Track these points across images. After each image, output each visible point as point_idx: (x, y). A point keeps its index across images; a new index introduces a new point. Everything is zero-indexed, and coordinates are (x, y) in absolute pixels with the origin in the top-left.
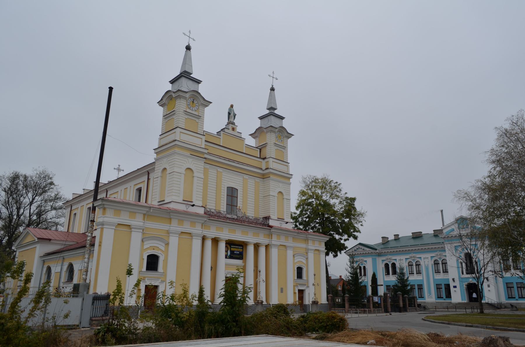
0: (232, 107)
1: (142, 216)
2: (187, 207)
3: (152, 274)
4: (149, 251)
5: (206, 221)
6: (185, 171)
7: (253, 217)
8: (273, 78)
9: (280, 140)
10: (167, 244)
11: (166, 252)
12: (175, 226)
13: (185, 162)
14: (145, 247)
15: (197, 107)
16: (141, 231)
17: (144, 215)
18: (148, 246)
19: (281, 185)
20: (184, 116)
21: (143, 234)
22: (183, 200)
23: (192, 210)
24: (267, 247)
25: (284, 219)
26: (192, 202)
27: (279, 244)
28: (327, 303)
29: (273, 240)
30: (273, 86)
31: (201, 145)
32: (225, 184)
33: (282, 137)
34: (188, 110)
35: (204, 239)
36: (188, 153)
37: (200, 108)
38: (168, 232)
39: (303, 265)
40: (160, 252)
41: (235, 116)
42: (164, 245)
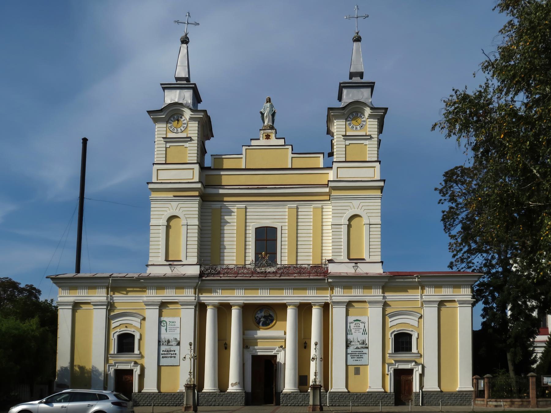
2: (173, 268)
3: (124, 357)
4: (118, 330)
7: (309, 265)
9: (358, 127)
10: (144, 319)
14: (113, 326)
15: (185, 125)
16: (105, 307)
18: (118, 324)
19: (356, 203)
24: (326, 308)
25: (364, 259)
26: (181, 261)
27: (348, 300)
28: (472, 389)
29: (334, 294)
34: (170, 135)
35: (201, 308)
36: (170, 195)
37: (189, 125)
39: (411, 329)
42: (139, 320)
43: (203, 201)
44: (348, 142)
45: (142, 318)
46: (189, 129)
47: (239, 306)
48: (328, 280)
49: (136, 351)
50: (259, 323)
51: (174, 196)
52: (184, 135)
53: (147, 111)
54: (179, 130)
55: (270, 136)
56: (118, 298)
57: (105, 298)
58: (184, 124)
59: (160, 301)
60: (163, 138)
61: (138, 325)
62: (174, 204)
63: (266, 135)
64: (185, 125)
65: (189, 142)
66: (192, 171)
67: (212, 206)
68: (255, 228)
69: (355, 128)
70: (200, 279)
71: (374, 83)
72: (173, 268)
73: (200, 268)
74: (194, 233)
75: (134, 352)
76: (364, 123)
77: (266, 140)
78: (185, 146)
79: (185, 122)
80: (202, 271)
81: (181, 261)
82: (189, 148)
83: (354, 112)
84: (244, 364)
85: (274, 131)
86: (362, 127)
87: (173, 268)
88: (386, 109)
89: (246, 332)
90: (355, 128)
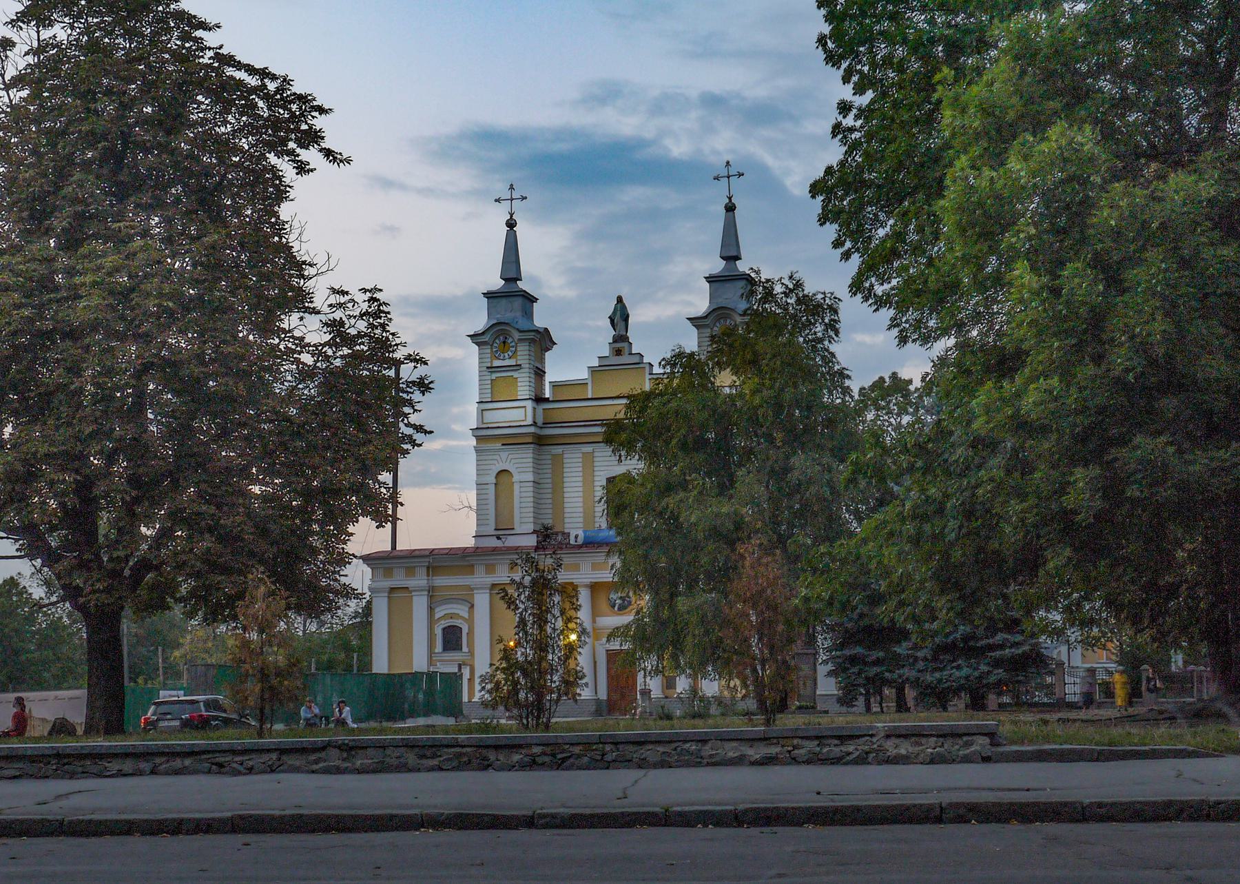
1: (425, 570)
4: (443, 622)
6: (496, 478)
10: (472, 606)
11: (470, 621)
12: (481, 578)
13: (495, 462)
14: (437, 616)
15: (514, 349)
16: (426, 593)
17: (428, 568)
20: (489, 377)
21: (431, 597)
22: (496, 529)
23: (512, 542)
30: (730, 198)
31: (525, 420)
32: (602, 473)
34: (497, 363)
36: (498, 445)
38: (470, 589)
40: (460, 621)
41: (626, 318)
42: (467, 609)
45: (470, 605)
46: (519, 353)
47: (586, 586)
49: (465, 649)
50: (613, 607)
51: (503, 445)
52: (512, 362)
54: (506, 355)
56: (440, 581)
57: (426, 581)
58: (513, 347)
59: (490, 583)
60: (488, 368)
61: (466, 616)
62: (504, 455)
64: (514, 349)
67: (553, 451)
74: (529, 488)
75: (461, 649)
79: (513, 344)
82: (519, 380)
84: (595, 663)
85: (625, 345)
89: (598, 619)
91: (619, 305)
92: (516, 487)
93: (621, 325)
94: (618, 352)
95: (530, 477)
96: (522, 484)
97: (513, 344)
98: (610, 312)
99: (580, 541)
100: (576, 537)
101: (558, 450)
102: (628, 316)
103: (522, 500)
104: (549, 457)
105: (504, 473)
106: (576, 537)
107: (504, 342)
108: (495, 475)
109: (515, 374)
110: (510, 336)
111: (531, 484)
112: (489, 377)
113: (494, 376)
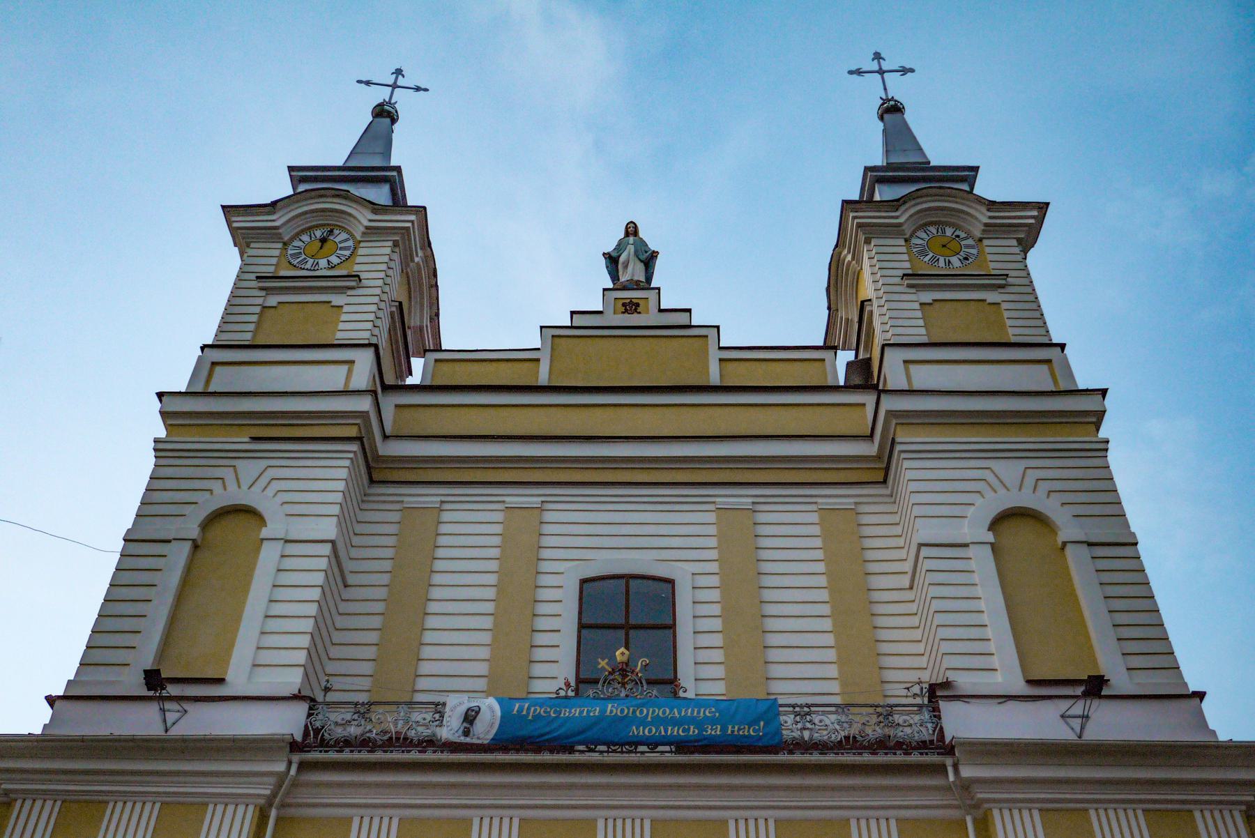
0: (636, 233)
5: (281, 777)
8: (881, 72)
15: (347, 253)
26: (221, 681)
33: (970, 242)
36: (240, 440)
41: (649, 260)
43: (372, 481)
44: (927, 297)
48: (956, 767)
51: (255, 439)
53: (223, 207)
55: (638, 305)
63: (624, 305)
64: (347, 253)
65: (350, 292)
66: (345, 368)
68: (584, 582)
69: (942, 259)
70: (296, 758)
71: (975, 169)
72: (177, 715)
73: (309, 715)
76: (974, 251)
77: (626, 315)
78: (332, 304)
80: (317, 731)
81: (221, 681)
82: (346, 309)
83: (931, 224)
85: (651, 295)
86: (966, 259)
87: (177, 715)
88: (1043, 207)
90: (942, 259)
91: (631, 239)
92: (269, 556)
93: (634, 271)
94: (631, 307)
95: (328, 529)
96: (292, 549)
97: (350, 243)
98: (610, 247)
99: (485, 730)
100: (470, 717)
101: (429, 497)
102: (654, 255)
103: (273, 625)
104: (395, 517)
105: (241, 520)
106: (470, 717)
107: (323, 241)
108: (203, 514)
109: (337, 300)
110: (342, 228)
111: (326, 549)
112: (260, 301)
113: (273, 300)
